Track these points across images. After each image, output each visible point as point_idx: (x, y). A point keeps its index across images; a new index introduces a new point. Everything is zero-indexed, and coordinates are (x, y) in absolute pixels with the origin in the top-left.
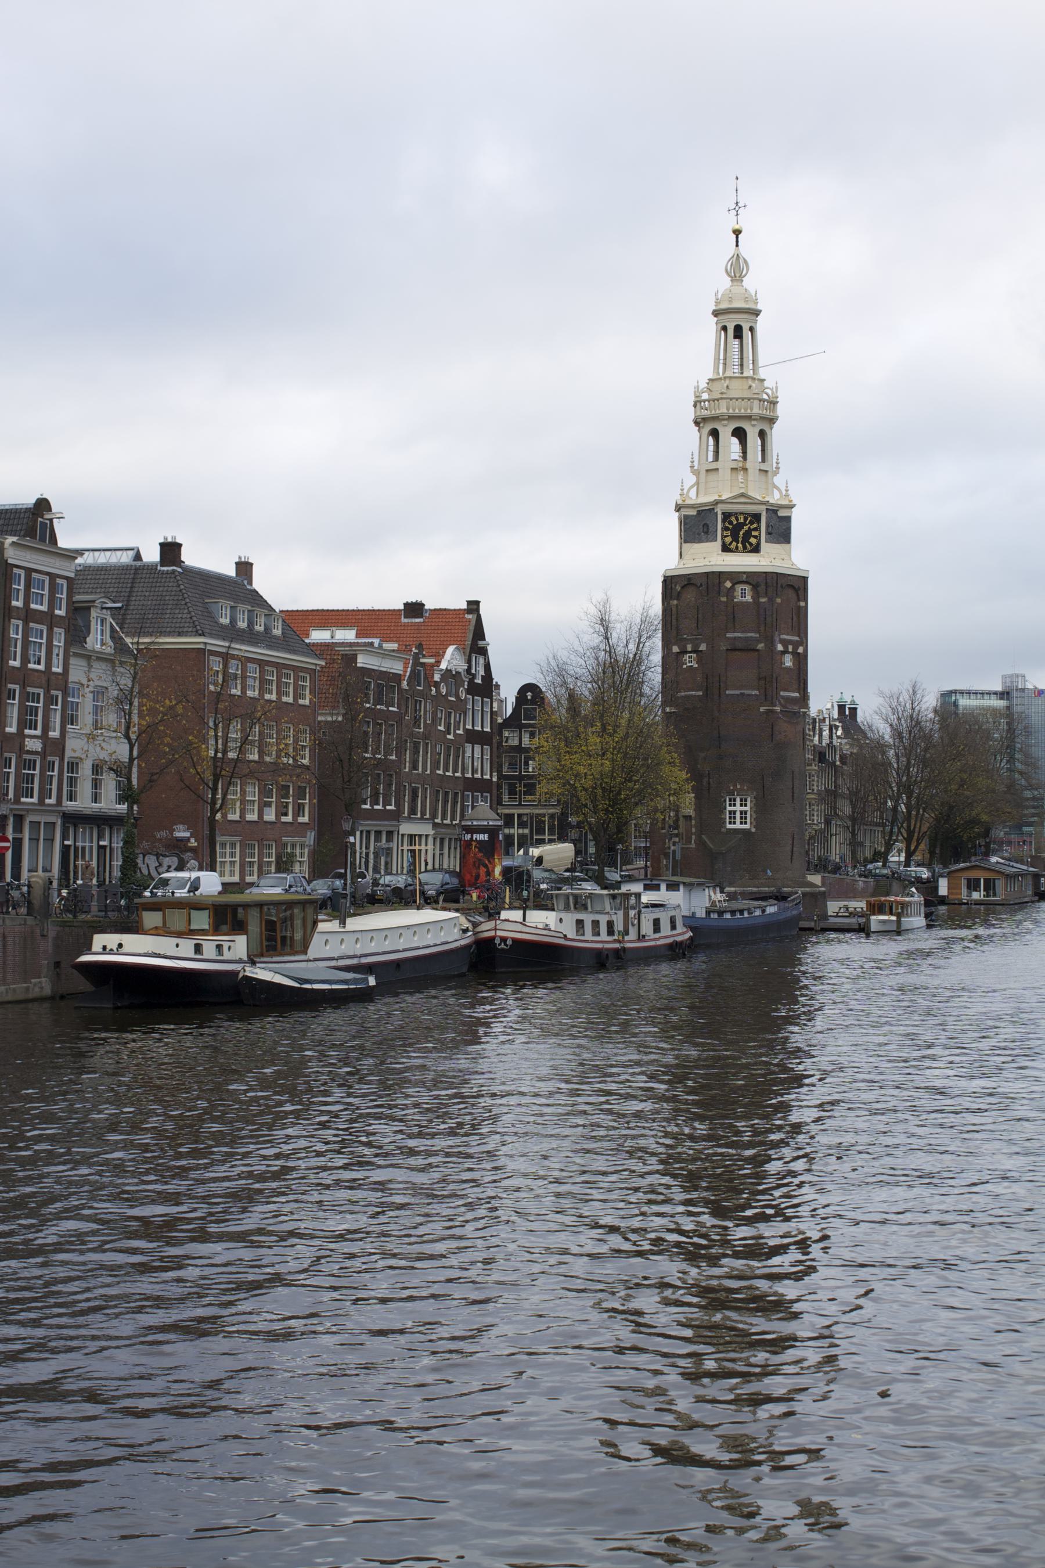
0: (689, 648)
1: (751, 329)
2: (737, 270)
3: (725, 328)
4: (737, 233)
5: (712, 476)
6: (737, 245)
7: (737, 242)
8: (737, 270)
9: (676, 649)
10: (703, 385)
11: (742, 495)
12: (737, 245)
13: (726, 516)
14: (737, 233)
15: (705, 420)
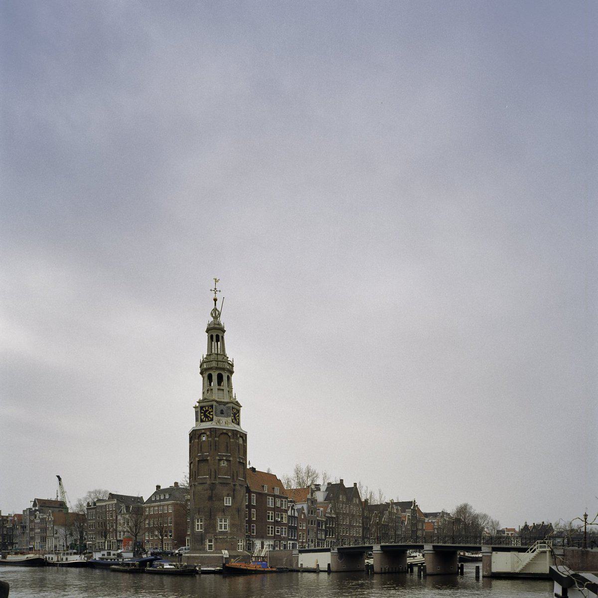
0: (224, 458)
1: (223, 337)
2: (216, 314)
3: (217, 336)
4: (215, 300)
5: (220, 392)
6: (215, 305)
7: (215, 304)
8: (216, 314)
9: (218, 458)
10: (205, 356)
11: (237, 402)
12: (215, 305)
13: (233, 408)
14: (215, 300)
15: (217, 368)
